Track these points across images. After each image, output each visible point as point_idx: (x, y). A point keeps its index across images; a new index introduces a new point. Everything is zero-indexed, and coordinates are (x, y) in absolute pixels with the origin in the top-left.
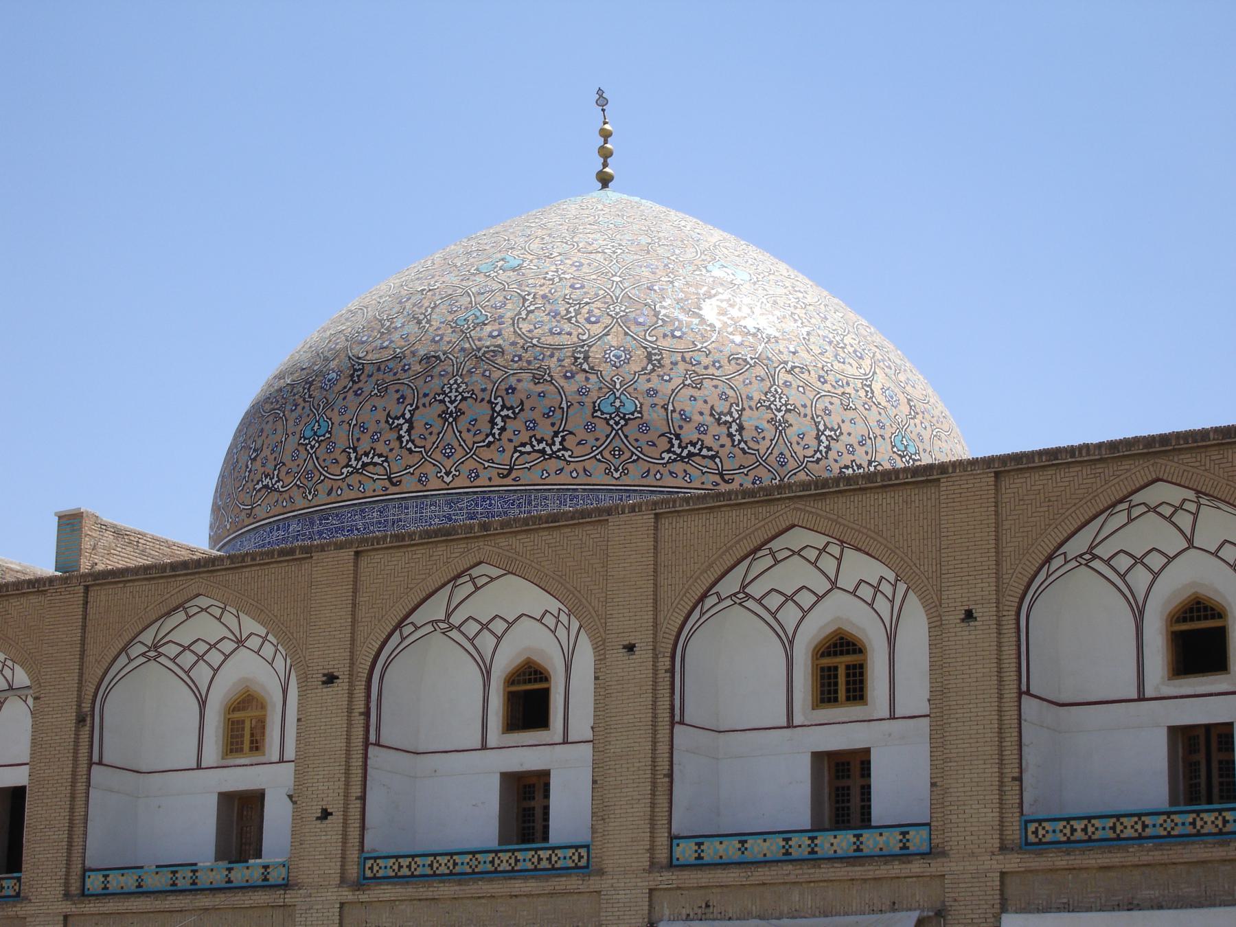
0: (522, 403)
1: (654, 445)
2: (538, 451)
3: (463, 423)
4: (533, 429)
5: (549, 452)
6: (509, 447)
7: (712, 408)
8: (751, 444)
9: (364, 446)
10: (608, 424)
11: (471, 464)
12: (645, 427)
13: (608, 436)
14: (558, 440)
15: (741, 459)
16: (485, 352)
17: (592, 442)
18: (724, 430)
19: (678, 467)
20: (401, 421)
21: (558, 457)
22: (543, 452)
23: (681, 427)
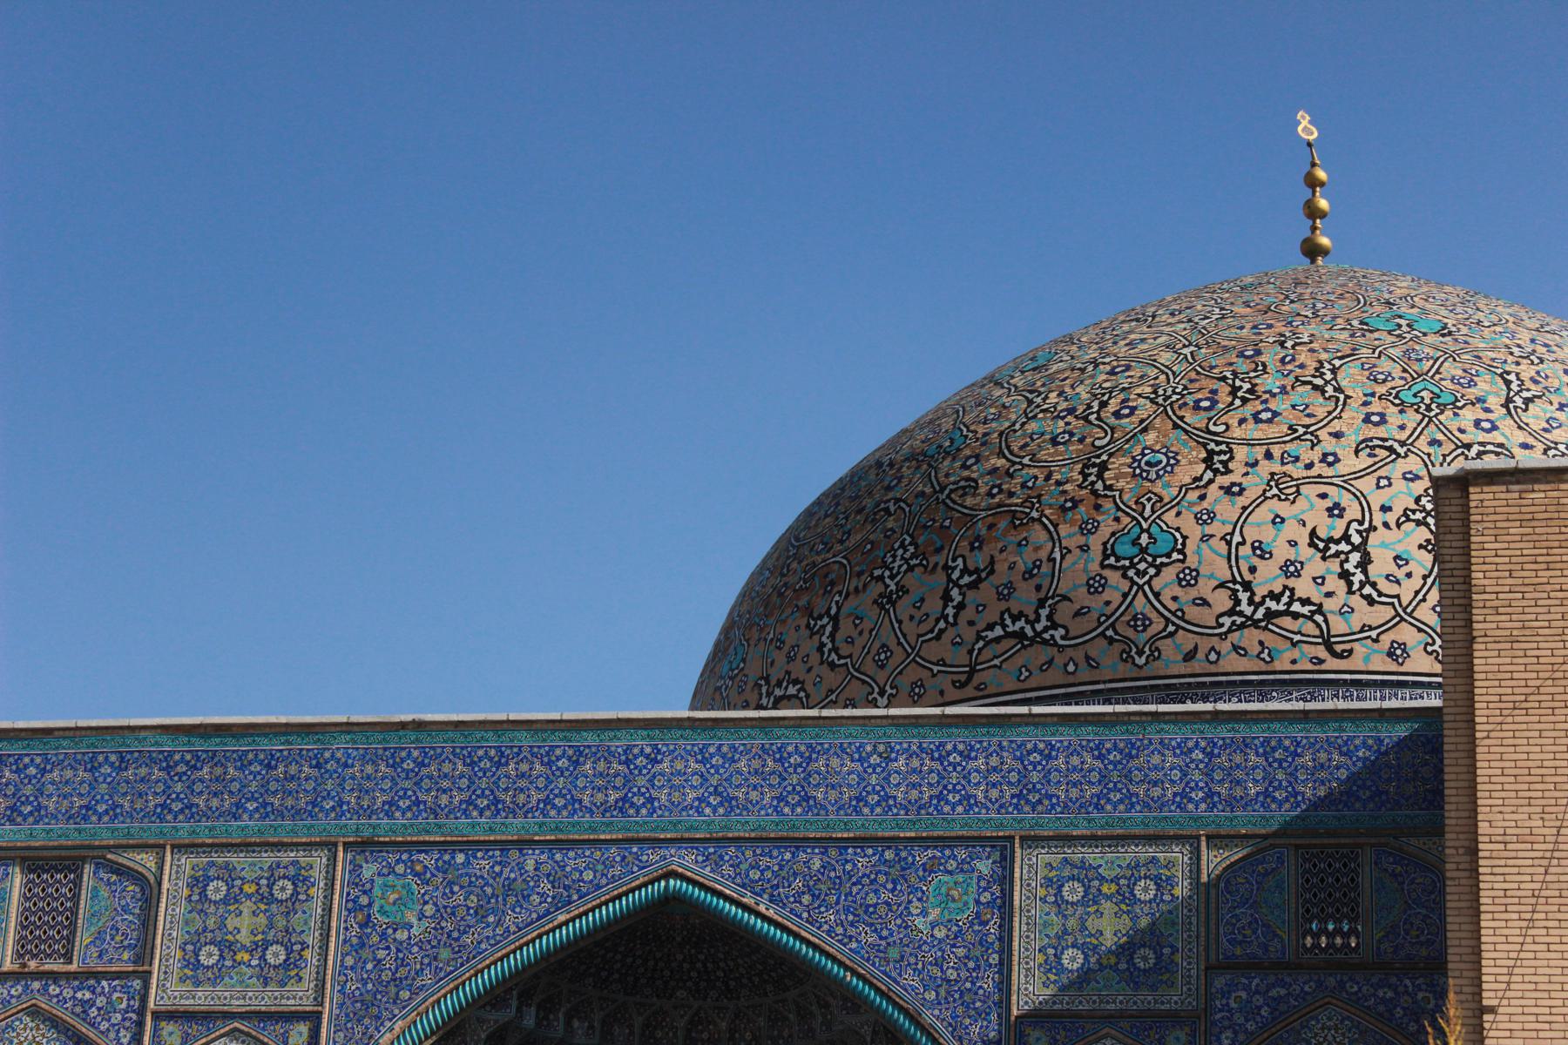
0: (992, 561)
1: (1205, 603)
2: (1013, 635)
3: (904, 607)
4: (1006, 598)
5: (1029, 632)
6: (969, 634)
7: (1313, 533)
8: (1384, 586)
9: (776, 674)
10: (1125, 576)
12: (1189, 578)
13: (1125, 596)
14: (1044, 612)
15: (1365, 614)
16: (952, 491)
18: (1334, 565)
19: (1250, 638)
20: (826, 620)
21: (1045, 642)
22: (1021, 635)
23: (1253, 570)
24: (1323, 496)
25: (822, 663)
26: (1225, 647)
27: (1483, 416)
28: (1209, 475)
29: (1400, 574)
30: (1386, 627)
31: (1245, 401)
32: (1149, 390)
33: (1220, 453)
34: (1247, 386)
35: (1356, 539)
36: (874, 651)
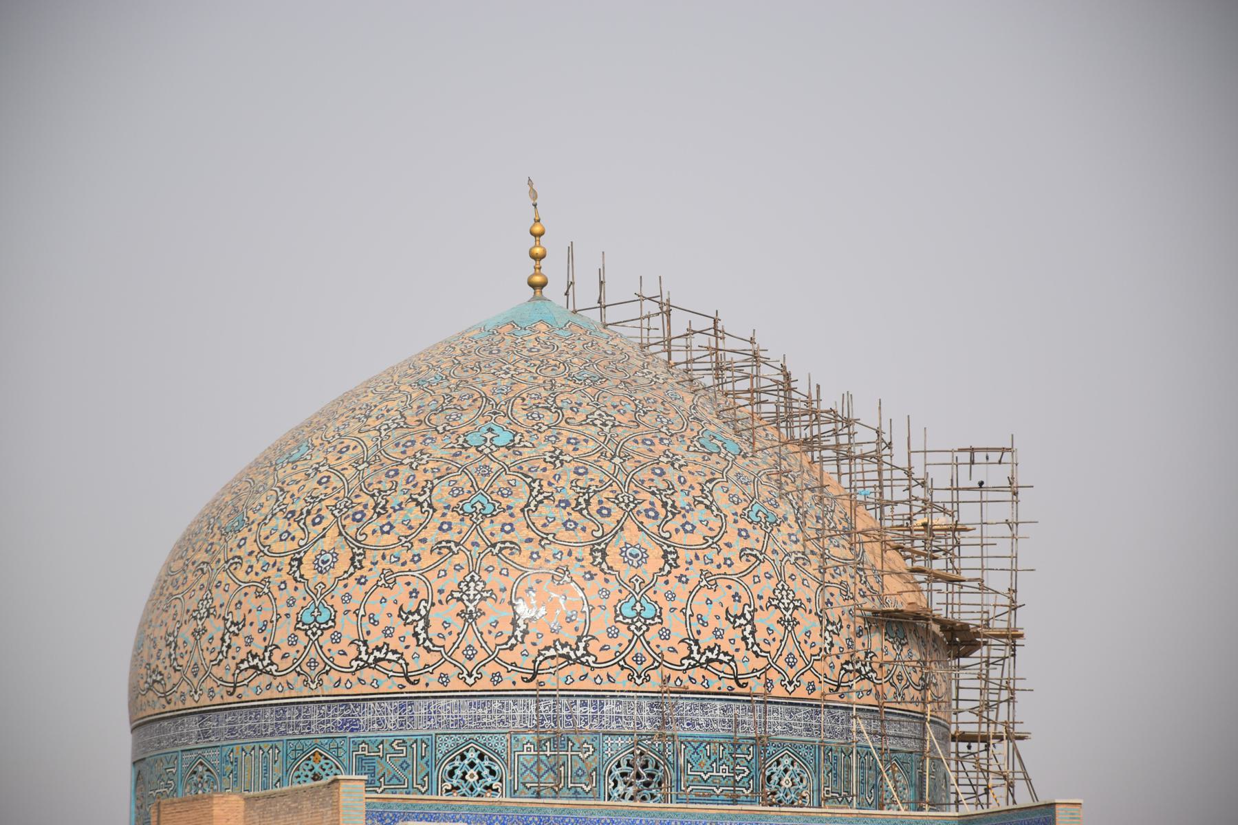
1: (675, 651)
2: (562, 656)
3: (483, 624)
5: (572, 654)
7: (727, 611)
10: (629, 629)
11: (492, 668)
12: (665, 635)
13: (630, 641)
16: (501, 549)
17: (615, 648)
18: (737, 634)
19: (697, 673)
20: (416, 617)
21: (582, 663)
22: (567, 657)
23: (699, 632)
24: (729, 587)
25: (418, 645)
26: (685, 677)
27: (790, 531)
28: (667, 568)
29: (770, 639)
30: (765, 670)
31: (674, 514)
32: (612, 495)
33: (671, 553)
34: (670, 503)
35: (748, 617)
36: (463, 647)
